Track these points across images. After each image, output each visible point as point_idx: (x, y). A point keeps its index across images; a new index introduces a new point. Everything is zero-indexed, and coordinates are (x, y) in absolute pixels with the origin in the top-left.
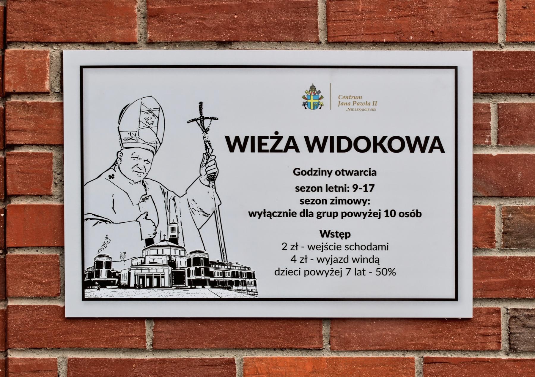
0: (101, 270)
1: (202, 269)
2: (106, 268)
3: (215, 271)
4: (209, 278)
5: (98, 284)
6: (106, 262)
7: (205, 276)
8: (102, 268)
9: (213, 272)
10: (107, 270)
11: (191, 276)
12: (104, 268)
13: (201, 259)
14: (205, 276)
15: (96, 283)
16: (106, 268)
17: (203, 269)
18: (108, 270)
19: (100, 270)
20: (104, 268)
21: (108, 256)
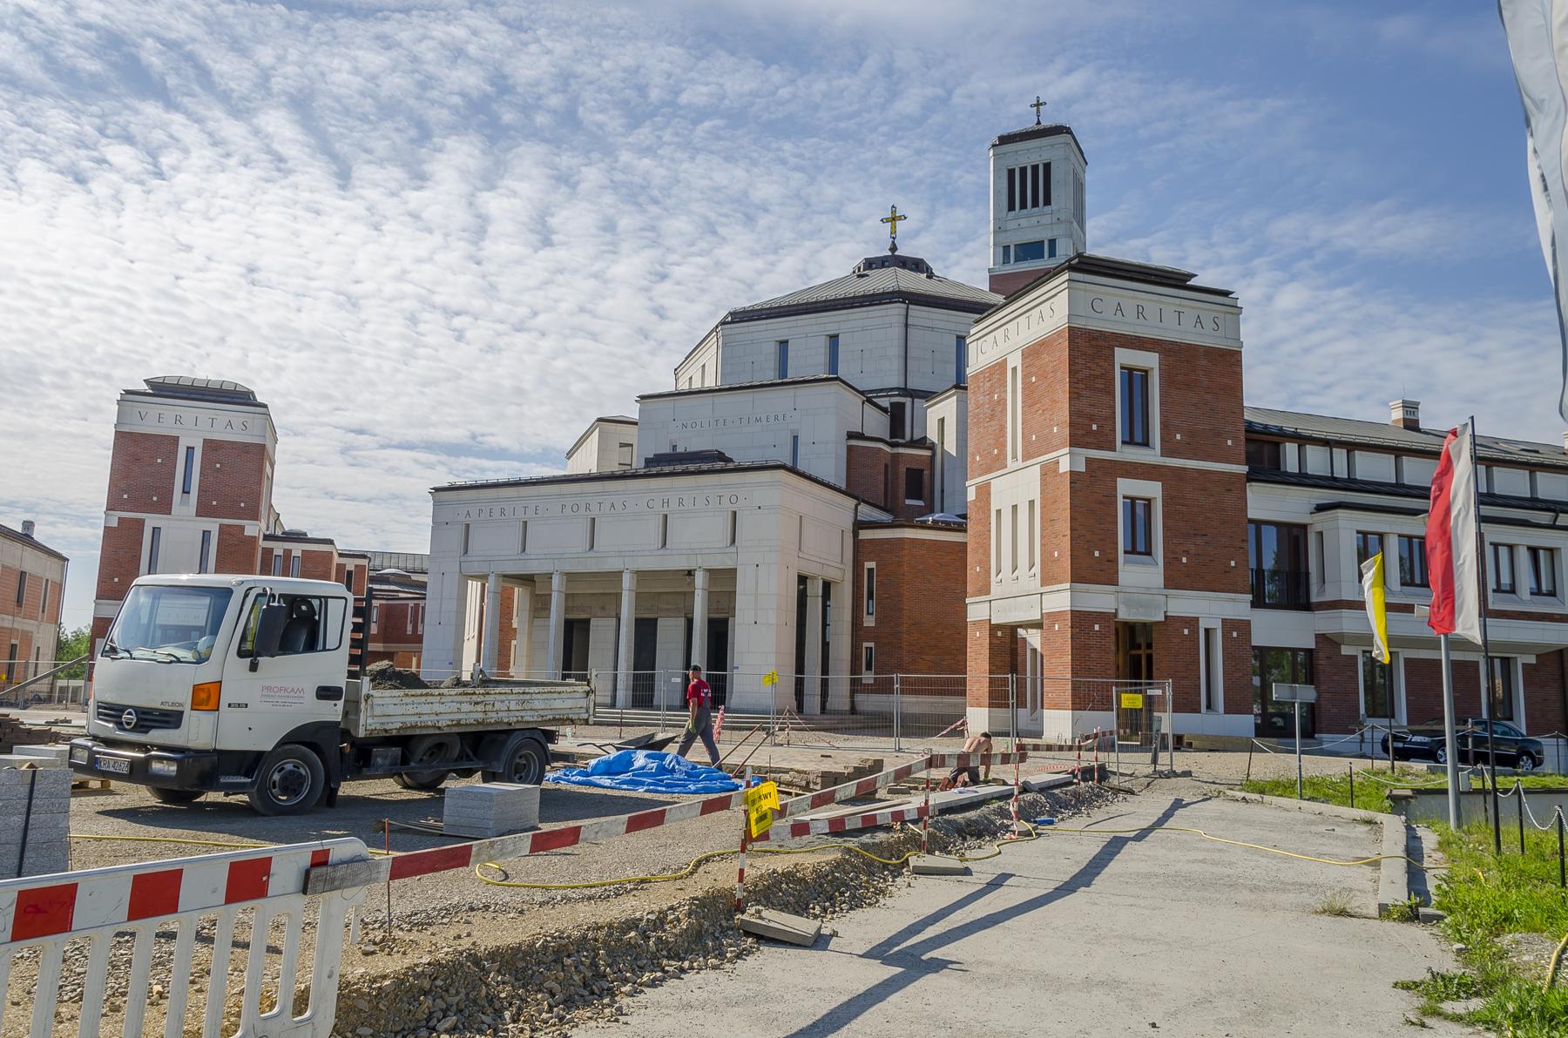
0: (151, 520)
1: (1127, 487)
2: (203, 510)
3: (1320, 522)
4: (1237, 606)
6: (211, 446)
7: (1176, 579)
8: (165, 507)
9: (1304, 528)
10: (213, 525)
11: (996, 590)
12: (184, 506)
13: (1123, 357)
14: (1176, 579)
16: (203, 510)
17: (1152, 489)
19: (141, 523)
20: (184, 506)
21: (240, 397)
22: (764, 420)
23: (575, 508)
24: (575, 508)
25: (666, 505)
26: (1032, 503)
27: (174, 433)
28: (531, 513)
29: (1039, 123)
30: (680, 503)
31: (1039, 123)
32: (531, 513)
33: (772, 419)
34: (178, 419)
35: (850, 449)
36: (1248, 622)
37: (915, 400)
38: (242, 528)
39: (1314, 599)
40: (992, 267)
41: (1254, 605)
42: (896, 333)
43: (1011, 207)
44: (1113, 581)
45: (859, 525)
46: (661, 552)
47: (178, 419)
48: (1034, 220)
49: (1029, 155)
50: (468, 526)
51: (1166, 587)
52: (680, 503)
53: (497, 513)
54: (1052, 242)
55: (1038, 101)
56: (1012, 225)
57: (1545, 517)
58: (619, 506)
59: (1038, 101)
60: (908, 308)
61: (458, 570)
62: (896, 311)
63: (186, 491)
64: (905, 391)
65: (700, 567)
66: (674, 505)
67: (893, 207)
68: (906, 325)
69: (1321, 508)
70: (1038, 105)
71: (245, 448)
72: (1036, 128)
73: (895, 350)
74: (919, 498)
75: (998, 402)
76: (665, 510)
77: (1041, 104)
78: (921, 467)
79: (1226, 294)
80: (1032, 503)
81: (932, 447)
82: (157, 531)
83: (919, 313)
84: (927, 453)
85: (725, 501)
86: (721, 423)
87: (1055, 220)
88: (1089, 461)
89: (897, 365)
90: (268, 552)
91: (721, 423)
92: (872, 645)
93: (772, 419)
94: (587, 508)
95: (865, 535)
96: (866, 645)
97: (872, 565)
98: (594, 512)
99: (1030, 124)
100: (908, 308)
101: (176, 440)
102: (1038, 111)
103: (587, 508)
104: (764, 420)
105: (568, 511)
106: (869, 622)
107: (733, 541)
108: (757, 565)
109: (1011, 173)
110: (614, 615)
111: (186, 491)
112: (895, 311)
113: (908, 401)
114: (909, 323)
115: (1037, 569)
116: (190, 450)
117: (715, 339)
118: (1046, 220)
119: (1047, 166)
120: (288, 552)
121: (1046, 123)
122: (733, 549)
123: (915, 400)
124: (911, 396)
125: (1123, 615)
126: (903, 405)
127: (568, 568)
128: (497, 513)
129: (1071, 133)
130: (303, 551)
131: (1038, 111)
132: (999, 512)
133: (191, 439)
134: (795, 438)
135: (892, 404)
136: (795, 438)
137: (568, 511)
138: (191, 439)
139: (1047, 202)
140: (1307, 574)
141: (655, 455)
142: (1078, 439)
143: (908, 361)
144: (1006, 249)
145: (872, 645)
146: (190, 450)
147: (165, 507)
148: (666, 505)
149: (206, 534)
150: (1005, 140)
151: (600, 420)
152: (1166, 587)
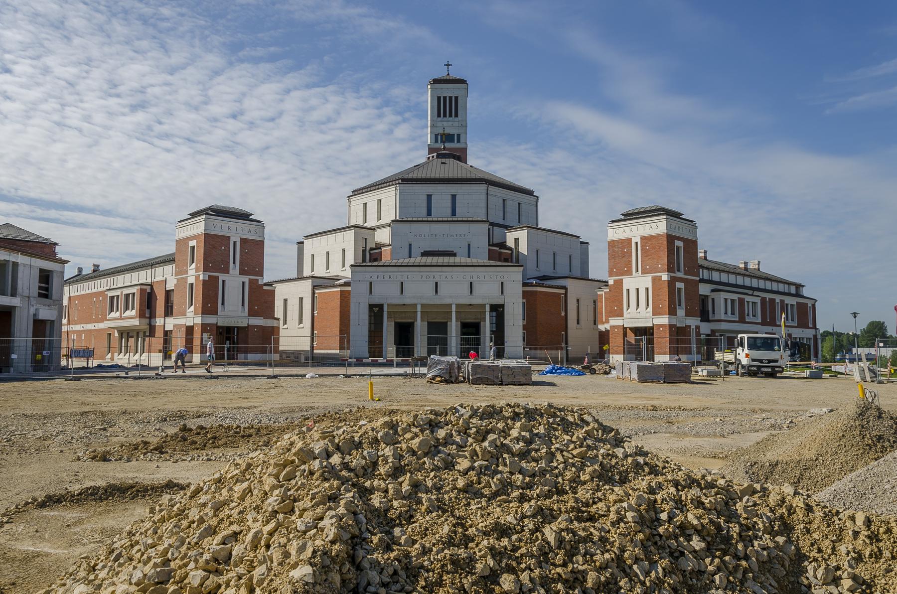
0: (222, 277)
2: (242, 272)
8: (226, 271)
9: (707, 296)
10: (246, 279)
12: (234, 269)
16: (242, 272)
19: (217, 277)
20: (234, 269)
21: (244, 216)
23: (428, 277)
24: (428, 277)
26: (647, 289)
29: (448, 74)
31: (448, 74)
33: (458, 236)
34: (229, 228)
35: (489, 249)
36: (699, 326)
39: (710, 319)
40: (429, 143)
41: (701, 321)
42: (484, 197)
43: (439, 116)
44: (676, 315)
46: (471, 297)
48: (450, 123)
49: (449, 91)
50: (371, 283)
51: (686, 316)
53: (387, 278)
54: (459, 136)
56: (440, 124)
57: (750, 292)
58: (449, 278)
60: (488, 187)
62: (483, 188)
68: (487, 194)
69: (713, 291)
72: (448, 78)
73: (484, 205)
75: (627, 252)
79: (692, 221)
80: (647, 289)
81: (510, 249)
82: (224, 281)
83: (492, 189)
84: (510, 252)
86: (434, 236)
88: (671, 277)
89: (484, 211)
91: (434, 236)
93: (458, 236)
94: (434, 277)
100: (488, 187)
103: (434, 277)
105: (424, 278)
107: (502, 293)
109: (439, 98)
112: (483, 187)
115: (650, 308)
118: (456, 124)
119: (456, 98)
121: (454, 75)
125: (678, 325)
127: (424, 302)
128: (387, 278)
132: (628, 290)
133: (235, 238)
134: (469, 245)
136: (469, 245)
137: (424, 278)
138: (235, 238)
139: (456, 116)
140: (708, 311)
142: (670, 269)
144: (436, 136)
147: (226, 271)
149: (244, 283)
150: (436, 81)
152: (686, 316)
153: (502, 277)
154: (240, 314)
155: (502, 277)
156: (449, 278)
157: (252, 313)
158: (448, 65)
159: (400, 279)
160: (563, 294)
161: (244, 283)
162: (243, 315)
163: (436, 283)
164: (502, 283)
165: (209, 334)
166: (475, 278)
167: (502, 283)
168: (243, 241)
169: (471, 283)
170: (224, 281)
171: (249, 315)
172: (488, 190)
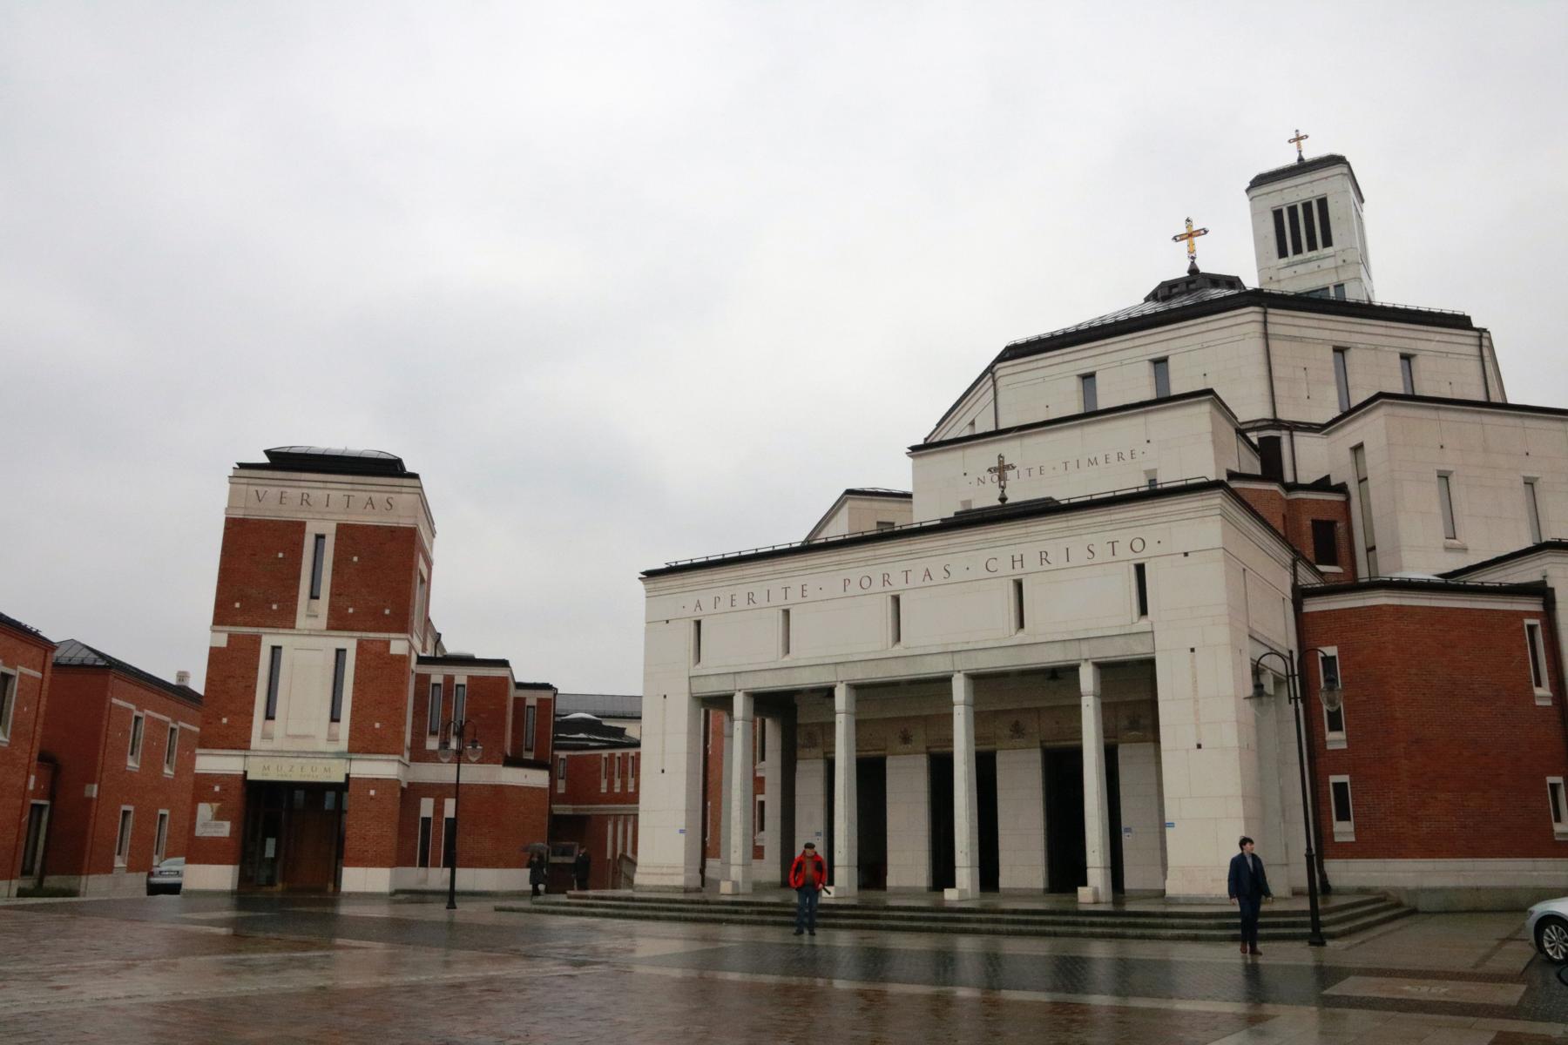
2: (338, 621)
5: (224, 829)
6: (344, 531)
8: (286, 619)
10: (349, 643)
12: (312, 612)
15: (205, 811)
16: (338, 621)
18: (361, 646)
19: (256, 640)
20: (312, 612)
22: (1101, 460)
23: (866, 582)
24: (866, 582)
25: (1018, 565)
27: (299, 516)
28: (794, 595)
30: (1043, 557)
32: (794, 595)
37: (1294, 433)
38: (387, 643)
42: (1256, 345)
43: (1282, 253)
45: (1300, 594)
47: (305, 500)
52: (1043, 557)
53: (741, 601)
55: (1298, 135)
58: (939, 575)
59: (1298, 135)
61: (687, 691)
63: (314, 596)
64: (1276, 423)
65: (1086, 660)
66: (1032, 563)
67: (1188, 220)
68: (1266, 336)
70: (1298, 139)
71: (393, 532)
74: (1333, 562)
76: (1018, 572)
77: (1302, 138)
78: (1332, 518)
82: (276, 650)
85: (1123, 551)
86: (1035, 472)
87: (1340, 263)
90: (423, 680)
91: (1035, 472)
92: (1345, 778)
94: (886, 580)
95: (1313, 606)
96: (1334, 779)
97: (1331, 651)
98: (898, 584)
99: (1292, 160)
101: (300, 527)
102: (1299, 146)
103: (886, 580)
104: (1101, 460)
105: (853, 588)
106: (1336, 740)
107: (1143, 610)
108: (1192, 650)
109: (1278, 214)
110: (924, 749)
111: (314, 596)
112: (1251, 315)
113: (1284, 436)
114: (1269, 332)
116: (320, 538)
117: (991, 382)
119: (1323, 203)
120: (449, 679)
122: (1144, 624)
123: (1294, 433)
124: (1287, 428)
126: (1277, 440)
127: (862, 675)
128: (741, 601)
129: (1348, 164)
130: (469, 677)
131: (1299, 146)
135: (1260, 439)
137: (853, 588)
139: (1328, 242)
141: (956, 513)
143: (1275, 383)
145: (1345, 778)
146: (320, 538)
147: (286, 619)
148: (1018, 565)
149: (340, 653)
151: (849, 492)
153: (1138, 545)
154: (323, 746)
155: (1138, 545)
156: (939, 575)
157: (363, 743)
158: (1298, 139)
159: (779, 600)
160: (1530, 614)
161: (340, 653)
162: (333, 748)
163: (896, 600)
164: (1140, 569)
165: (216, 805)
166: (1032, 563)
167: (1140, 569)
168: (344, 531)
169: (1019, 585)
170: (276, 650)
171: (352, 750)
172: (1265, 323)
